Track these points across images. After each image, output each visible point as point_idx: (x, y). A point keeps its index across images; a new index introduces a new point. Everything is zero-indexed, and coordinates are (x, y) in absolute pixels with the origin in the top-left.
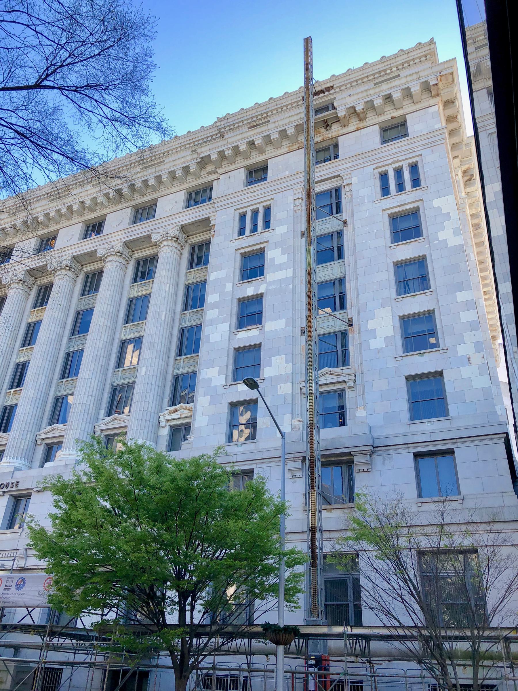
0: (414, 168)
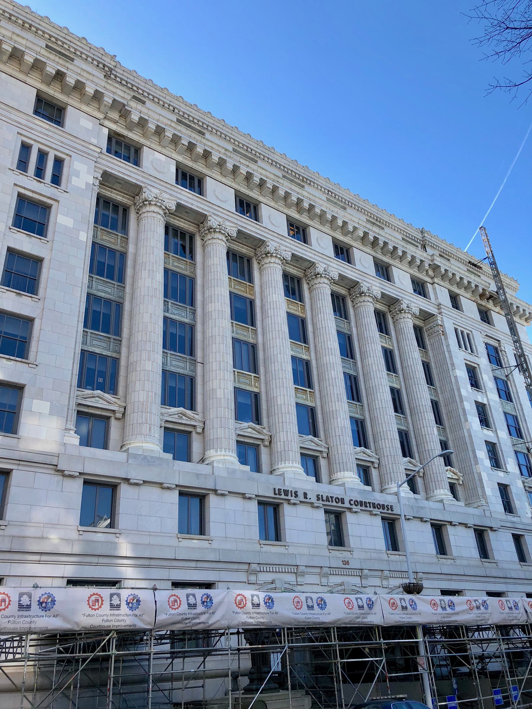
0: (59, 163)
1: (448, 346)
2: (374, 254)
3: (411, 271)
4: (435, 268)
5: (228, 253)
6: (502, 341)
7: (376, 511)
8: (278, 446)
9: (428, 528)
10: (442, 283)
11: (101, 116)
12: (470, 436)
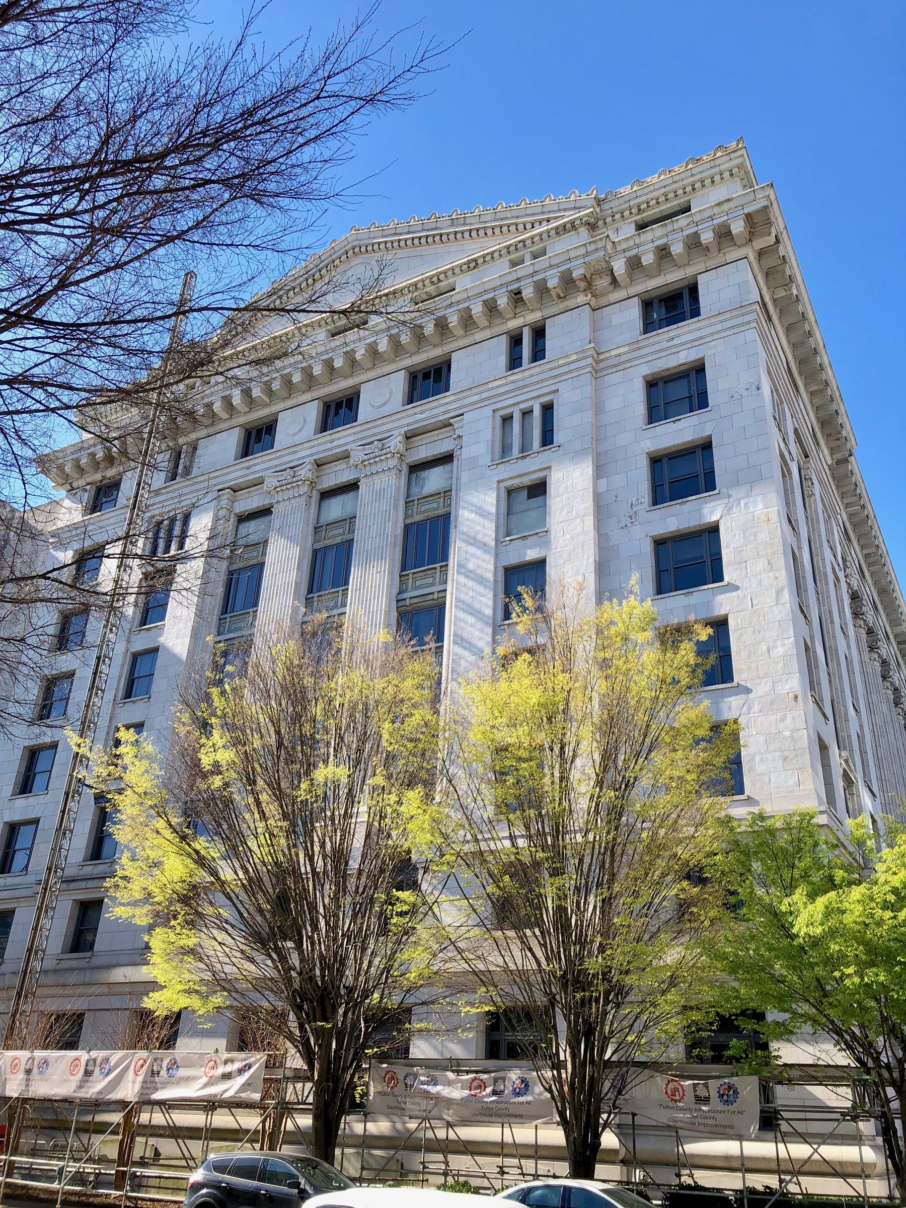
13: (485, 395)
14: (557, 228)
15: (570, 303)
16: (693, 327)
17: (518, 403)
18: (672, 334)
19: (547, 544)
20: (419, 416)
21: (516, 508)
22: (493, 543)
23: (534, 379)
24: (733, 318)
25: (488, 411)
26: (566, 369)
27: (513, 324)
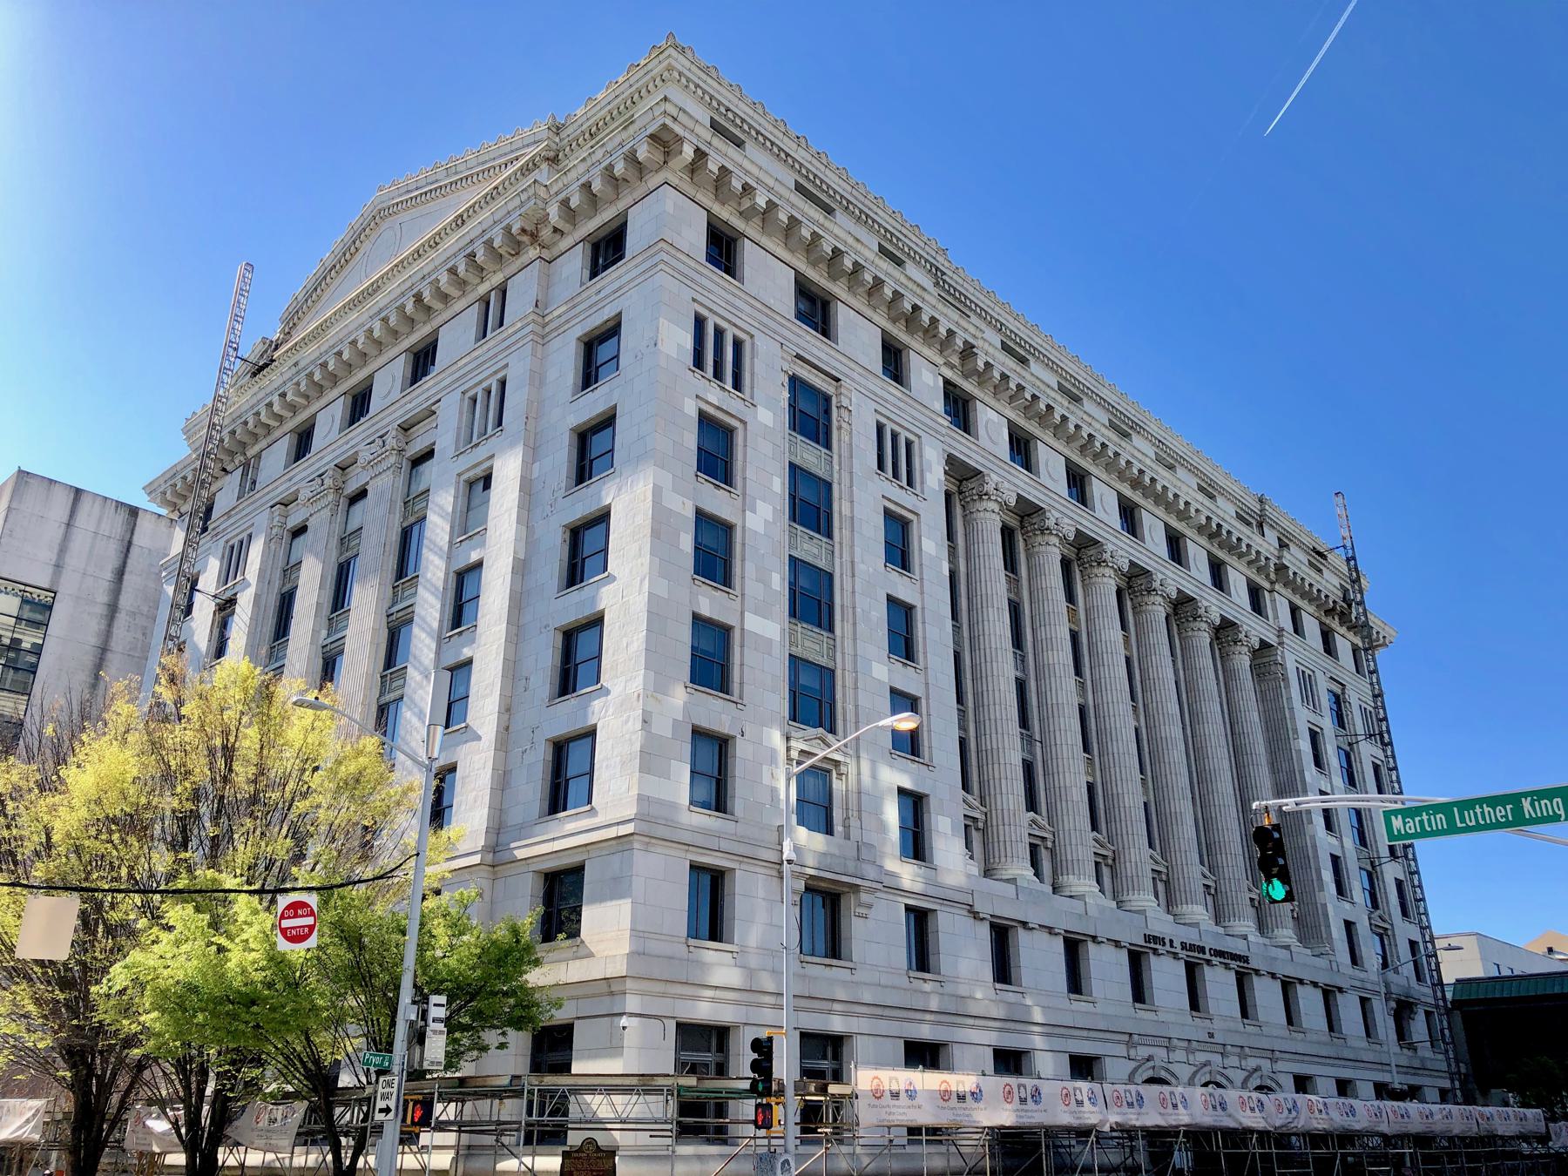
1: (1289, 698)
2: (1208, 546)
3: (1249, 573)
4: (1281, 569)
5: (1002, 530)
6: (1348, 686)
7: (1234, 964)
8: (1129, 869)
9: (1124, 957)
10: (1283, 591)
11: (939, 360)
12: (1315, 847)
13: (457, 375)
14: (521, 168)
15: (524, 259)
16: (614, 275)
17: (481, 382)
18: (598, 286)
19: (483, 544)
20: (409, 406)
21: (473, 504)
22: (446, 548)
23: (491, 353)
24: (644, 261)
25: (457, 395)
26: (513, 339)
27: (483, 289)
